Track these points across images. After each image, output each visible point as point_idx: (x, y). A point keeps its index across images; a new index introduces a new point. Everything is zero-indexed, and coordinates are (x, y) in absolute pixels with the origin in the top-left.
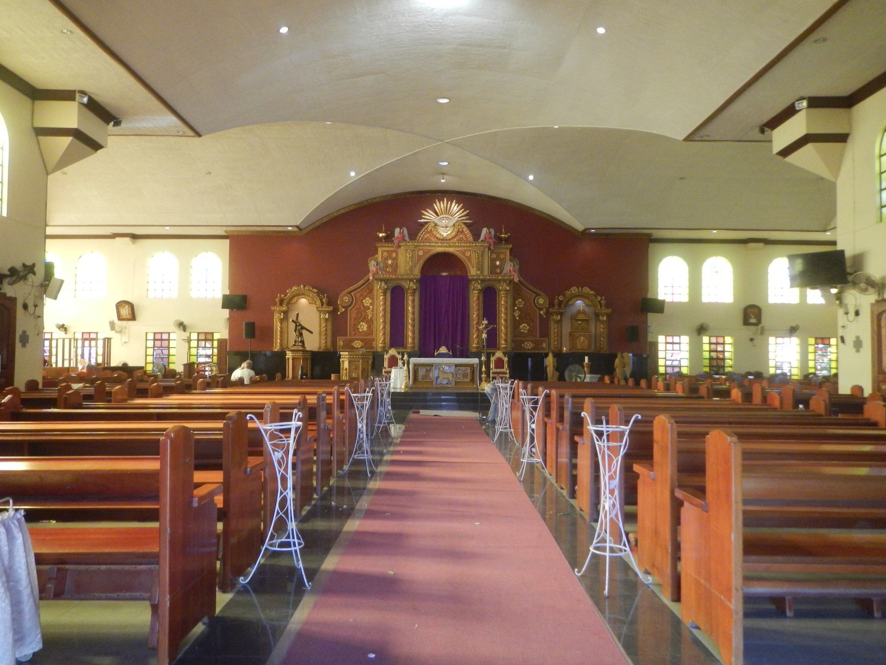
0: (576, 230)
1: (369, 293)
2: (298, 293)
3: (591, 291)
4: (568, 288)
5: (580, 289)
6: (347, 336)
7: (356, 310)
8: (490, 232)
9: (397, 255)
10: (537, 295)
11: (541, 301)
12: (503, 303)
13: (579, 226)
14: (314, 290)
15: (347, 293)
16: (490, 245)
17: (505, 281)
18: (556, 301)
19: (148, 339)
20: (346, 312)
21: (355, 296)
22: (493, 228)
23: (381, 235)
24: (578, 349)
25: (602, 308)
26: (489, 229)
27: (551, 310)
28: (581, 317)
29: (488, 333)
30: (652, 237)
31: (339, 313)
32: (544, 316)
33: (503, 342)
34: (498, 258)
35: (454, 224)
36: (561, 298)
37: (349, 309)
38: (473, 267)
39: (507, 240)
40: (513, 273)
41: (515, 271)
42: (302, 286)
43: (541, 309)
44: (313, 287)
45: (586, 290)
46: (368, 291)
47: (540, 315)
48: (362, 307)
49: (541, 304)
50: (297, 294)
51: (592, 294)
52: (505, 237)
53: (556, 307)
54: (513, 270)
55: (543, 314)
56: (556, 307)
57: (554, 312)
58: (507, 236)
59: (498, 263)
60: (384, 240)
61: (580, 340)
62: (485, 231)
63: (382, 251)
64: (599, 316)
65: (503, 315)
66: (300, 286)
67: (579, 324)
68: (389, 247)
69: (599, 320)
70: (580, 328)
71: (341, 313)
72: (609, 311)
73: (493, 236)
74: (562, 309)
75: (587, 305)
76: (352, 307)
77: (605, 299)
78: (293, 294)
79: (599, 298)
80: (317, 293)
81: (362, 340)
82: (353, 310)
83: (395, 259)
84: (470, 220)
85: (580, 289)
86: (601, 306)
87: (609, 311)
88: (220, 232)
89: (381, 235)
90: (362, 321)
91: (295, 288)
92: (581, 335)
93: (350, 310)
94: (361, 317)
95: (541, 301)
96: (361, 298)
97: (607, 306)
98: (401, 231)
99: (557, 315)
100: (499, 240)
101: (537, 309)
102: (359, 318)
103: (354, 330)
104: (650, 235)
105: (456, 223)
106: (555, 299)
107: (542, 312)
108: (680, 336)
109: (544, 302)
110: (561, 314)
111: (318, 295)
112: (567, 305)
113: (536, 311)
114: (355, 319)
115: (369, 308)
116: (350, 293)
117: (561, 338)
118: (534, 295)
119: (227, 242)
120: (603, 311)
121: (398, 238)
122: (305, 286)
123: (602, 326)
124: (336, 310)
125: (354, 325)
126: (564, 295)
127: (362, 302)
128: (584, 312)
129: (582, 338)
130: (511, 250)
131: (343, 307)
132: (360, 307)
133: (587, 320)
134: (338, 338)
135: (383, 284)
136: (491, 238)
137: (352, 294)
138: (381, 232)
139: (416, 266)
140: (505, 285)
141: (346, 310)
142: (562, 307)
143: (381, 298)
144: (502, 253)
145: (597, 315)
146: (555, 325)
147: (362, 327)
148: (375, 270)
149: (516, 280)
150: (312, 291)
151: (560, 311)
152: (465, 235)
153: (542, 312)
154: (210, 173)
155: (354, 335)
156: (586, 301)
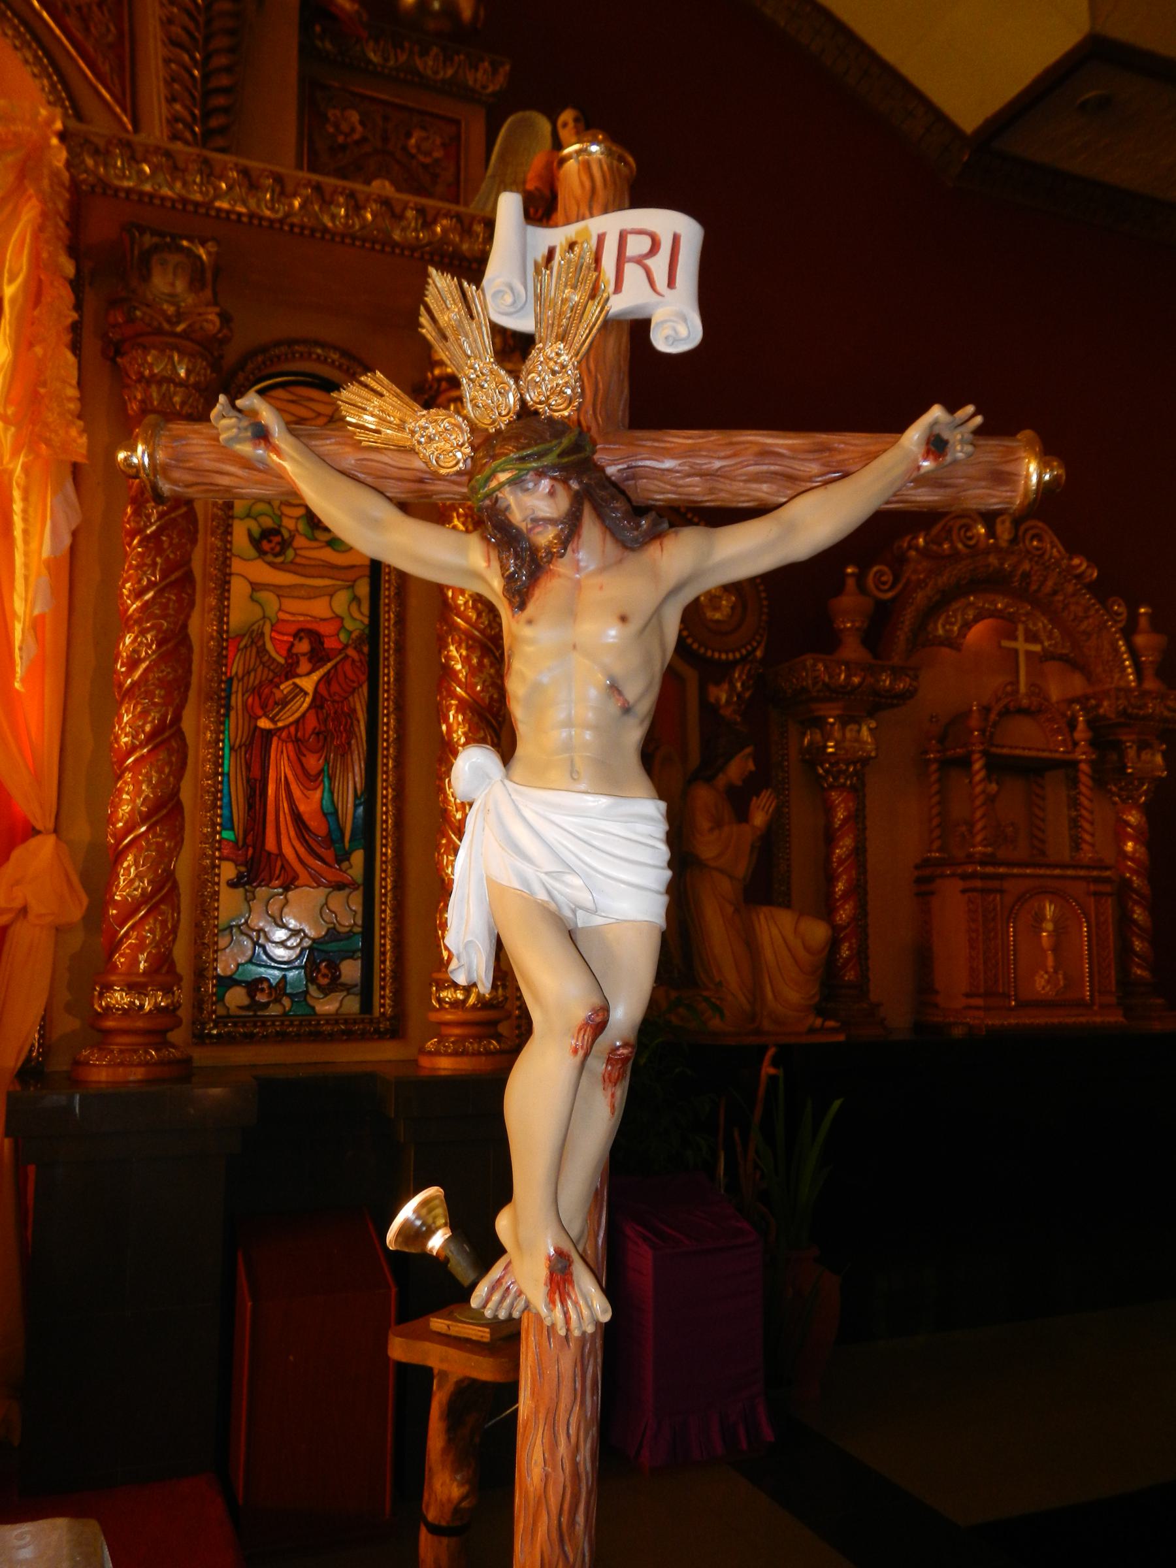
0: (939, 117)
3: (1072, 550)
24: (1023, 1005)
47: (709, 710)
55: (727, 712)
56: (852, 650)
57: (835, 693)
74: (897, 673)
77: (1156, 625)
106: (839, 590)
107: (720, 694)
123: (1133, 818)
126: (898, 563)
146: (829, 810)
151: (886, 681)
153: (720, 694)
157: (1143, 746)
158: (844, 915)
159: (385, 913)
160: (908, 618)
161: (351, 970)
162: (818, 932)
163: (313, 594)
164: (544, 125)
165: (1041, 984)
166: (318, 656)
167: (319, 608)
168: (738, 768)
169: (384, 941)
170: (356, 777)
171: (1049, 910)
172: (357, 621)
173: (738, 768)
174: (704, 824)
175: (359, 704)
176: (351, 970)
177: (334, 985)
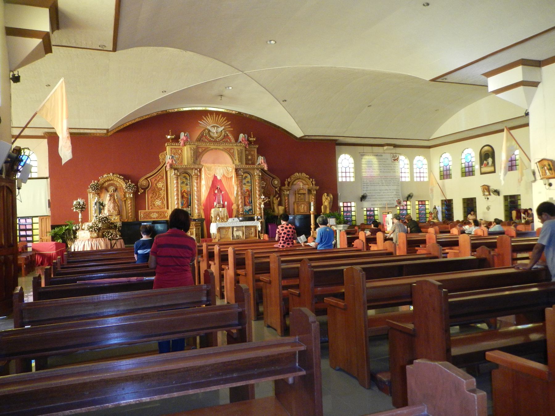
1: (162, 179)
2: (108, 179)
4: (293, 174)
5: (300, 174)
6: (146, 210)
7: (152, 191)
8: (245, 137)
9: (182, 151)
10: (274, 178)
11: (276, 182)
12: (257, 184)
13: (298, 133)
14: (121, 177)
15: (145, 179)
16: (246, 145)
17: (257, 169)
18: (286, 183)
19: (33, 218)
20: (144, 192)
21: (151, 181)
22: (247, 134)
23: (169, 137)
25: (314, 186)
26: (244, 134)
27: (283, 188)
28: (302, 192)
29: (265, 204)
30: (337, 142)
31: (139, 194)
32: (278, 192)
33: (258, 209)
34: (250, 154)
35: (221, 131)
36: (289, 180)
37: (147, 190)
38: (236, 160)
39: (255, 143)
40: (263, 164)
41: (264, 163)
42: (111, 174)
43: (276, 188)
44: (120, 175)
45: (304, 175)
46: (160, 177)
47: (276, 191)
48: (156, 188)
49: (276, 184)
50: (107, 180)
51: (307, 177)
52: (253, 140)
53: (286, 186)
54: (263, 162)
56: (286, 186)
58: (255, 139)
59: (250, 157)
60: (171, 141)
61: (302, 207)
62: (241, 135)
63: (171, 148)
64: (311, 191)
65: (257, 192)
66: (109, 174)
67: (299, 196)
68: (176, 146)
69: (311, 193)
70: (300, 199)
71: (141, 193)
72: (318, 188)
73: (247, 139)
75: (304, 184)
76: (149, 188)
77: (315, 181)
78: (104, 180)
79: (311, 180)
80: (123, 179)
81: (158, 212)
82: (150, 191)
83: (181, 154)
84: (231, 128)
85: (300, 174)
86: (313, 185)
87: (318, 188)
88: (40, 133)
89: (169, 137)
90: (156, 199)
91: (105, 176)
92: (302, 204)
93: (148, 191)
94: (156, 196)
95: (276, 182)
96: (155, 182)
97: (316, 185)
98: (186, 135)
99: (287, 191)
100: (250, 143)
101: (274, 188)
102: (155, 197)
103: (151, 205)
104: (336, 140)
105: (224, 129)
106: (285, 181)
107: (276, 189)
108: (351, 202)
109: (278, 183)
110: (289, 190)
111: (124, 180)
112: (292, 184)
113: (273, 189)
114: (151, 198)
115: (162, 190)
116: (146, 179)
117: (289, 206)
118: (272, 178)
119: (46, 141)
120: (314, 188)
121: (183, 139)
122: (113, 174)
124: (138, 191)
125: (151, 201)
127: (156, 185)
128: (303, 189)
129: (303, 205)
130: (258, 149)
131: (142, 189)
132: (155, 189)
133: (304, 194)
134: (139, 211)
135: (176, 172)
136: (245, 141)
137: (149, 179)
138: (169, 135)
139: (197, 159)
140: (258, 172)
141: (145, 192)
142: (290, 186)
143: (175, 182)
144: (252, 151)
145: (310, 191)
147: (157, 203)
148: (170, 162)
149: (266, 169)
150: (119, 178)
152: (229, 139)
153: (276, 189)
154: (49, 85)
155: (152, 209)
156: (304, 182)
157: (314, 191)
158: (287, 206)
159: (253, 207)
160: (291, 183)
161: (251, 211)
162: (283, 208)
163: (247, 187)
164: (261, 157)
165: (302, 211)
166: (248, 191)
167: (248, 188)
168: (277, 196)
169: (253, 209)
170: (251, 199)
171: (303, 205)
172: (250, 189)
173: (277, 196)
174: (274, 200)
175: (251, 194)
176: (251, 211)
177: (250, 212)
